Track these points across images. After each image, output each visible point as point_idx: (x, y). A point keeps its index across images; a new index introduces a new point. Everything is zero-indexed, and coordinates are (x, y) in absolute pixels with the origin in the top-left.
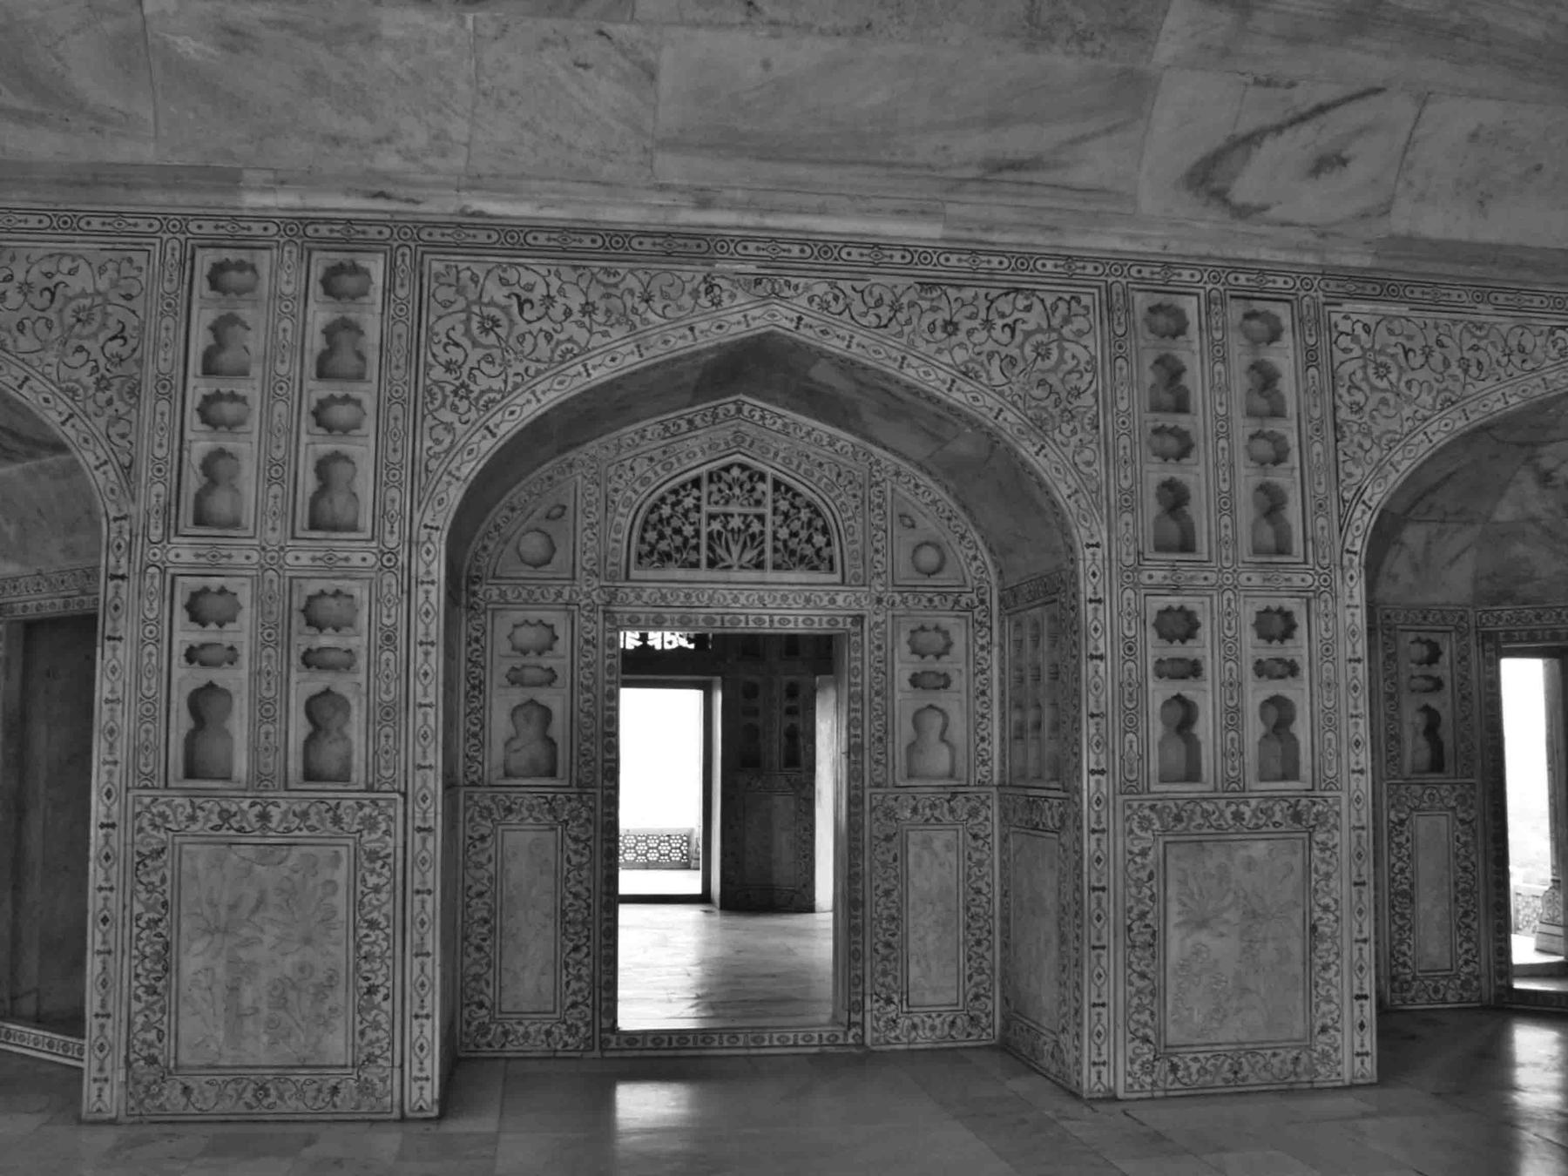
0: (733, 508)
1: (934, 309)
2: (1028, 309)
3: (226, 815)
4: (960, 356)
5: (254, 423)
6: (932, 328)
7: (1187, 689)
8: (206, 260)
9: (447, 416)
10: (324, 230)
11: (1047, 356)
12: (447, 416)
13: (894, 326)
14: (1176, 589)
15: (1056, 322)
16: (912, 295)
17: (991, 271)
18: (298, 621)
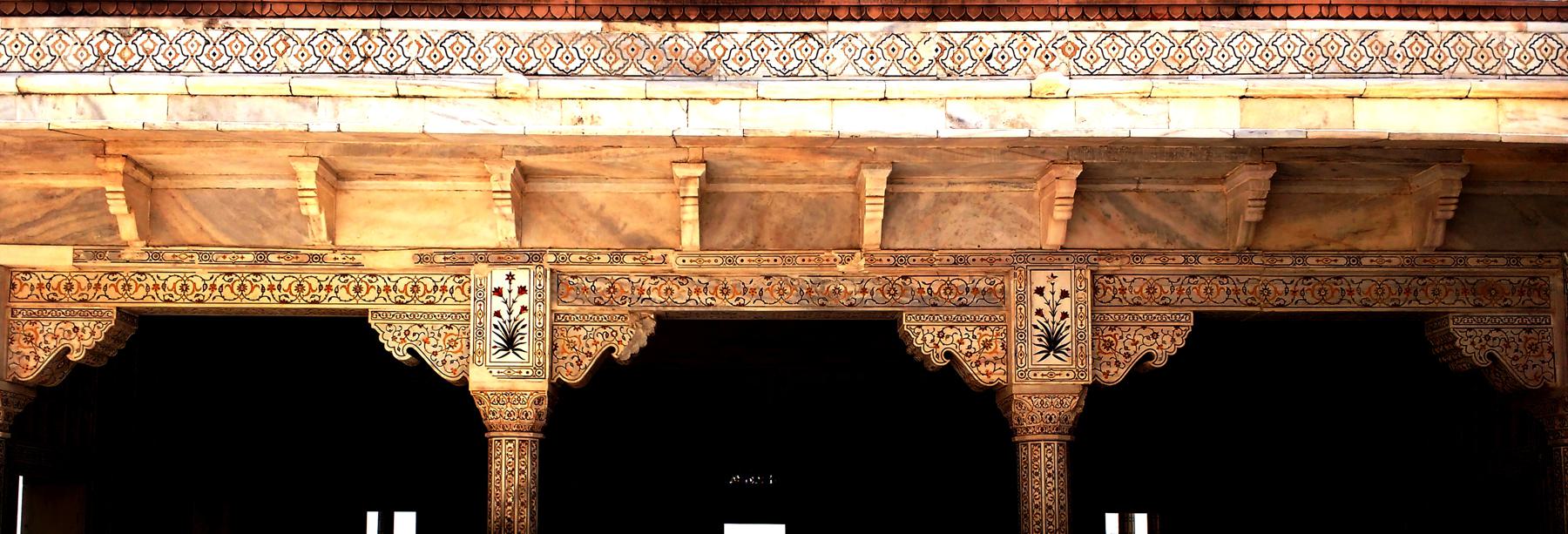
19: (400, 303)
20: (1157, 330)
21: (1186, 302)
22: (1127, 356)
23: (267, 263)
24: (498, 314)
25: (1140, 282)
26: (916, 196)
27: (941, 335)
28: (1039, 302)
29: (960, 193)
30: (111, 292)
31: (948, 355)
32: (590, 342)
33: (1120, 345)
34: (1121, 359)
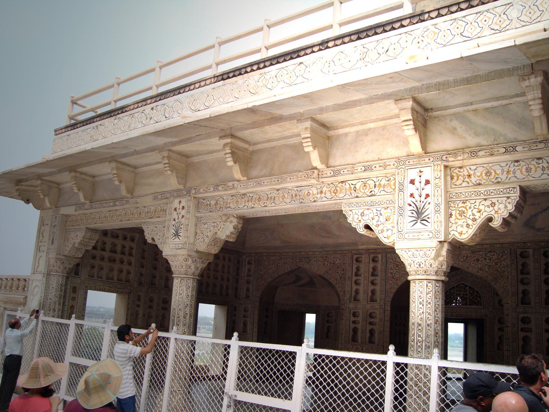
0: (461, 293)
1: (474, 257)
2: (494, 255)
3: (357, 348)
4: (479, 266)
5: (362, 284)
6: (474, 260)
7: (528, 334)
8: (355, 257)
9: (391, 282)
10: (371, 251)
11: (498, 264)
12: (391, 282)
13: (467, 261)
14: (525, 313)
15: (499, 257)
16: (470, 254)
17: (486, 248)
18: (368, 317)
19: (151, 218)
20: (494, 200)
21: (514, 179)
22: (474, 220)
23: (116, 206)
24: (174, 220)
25: (480, 169)
26: (346, 135)
27: (362, 214)
28: (411, 189)
29: (369, 129)
30: (85, 222)
31: (367, 227)
32: (209, 230)
33: (470, 212)
34: (470, 222)
